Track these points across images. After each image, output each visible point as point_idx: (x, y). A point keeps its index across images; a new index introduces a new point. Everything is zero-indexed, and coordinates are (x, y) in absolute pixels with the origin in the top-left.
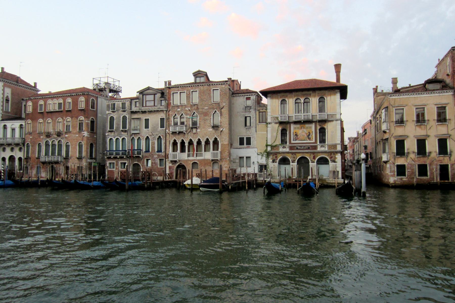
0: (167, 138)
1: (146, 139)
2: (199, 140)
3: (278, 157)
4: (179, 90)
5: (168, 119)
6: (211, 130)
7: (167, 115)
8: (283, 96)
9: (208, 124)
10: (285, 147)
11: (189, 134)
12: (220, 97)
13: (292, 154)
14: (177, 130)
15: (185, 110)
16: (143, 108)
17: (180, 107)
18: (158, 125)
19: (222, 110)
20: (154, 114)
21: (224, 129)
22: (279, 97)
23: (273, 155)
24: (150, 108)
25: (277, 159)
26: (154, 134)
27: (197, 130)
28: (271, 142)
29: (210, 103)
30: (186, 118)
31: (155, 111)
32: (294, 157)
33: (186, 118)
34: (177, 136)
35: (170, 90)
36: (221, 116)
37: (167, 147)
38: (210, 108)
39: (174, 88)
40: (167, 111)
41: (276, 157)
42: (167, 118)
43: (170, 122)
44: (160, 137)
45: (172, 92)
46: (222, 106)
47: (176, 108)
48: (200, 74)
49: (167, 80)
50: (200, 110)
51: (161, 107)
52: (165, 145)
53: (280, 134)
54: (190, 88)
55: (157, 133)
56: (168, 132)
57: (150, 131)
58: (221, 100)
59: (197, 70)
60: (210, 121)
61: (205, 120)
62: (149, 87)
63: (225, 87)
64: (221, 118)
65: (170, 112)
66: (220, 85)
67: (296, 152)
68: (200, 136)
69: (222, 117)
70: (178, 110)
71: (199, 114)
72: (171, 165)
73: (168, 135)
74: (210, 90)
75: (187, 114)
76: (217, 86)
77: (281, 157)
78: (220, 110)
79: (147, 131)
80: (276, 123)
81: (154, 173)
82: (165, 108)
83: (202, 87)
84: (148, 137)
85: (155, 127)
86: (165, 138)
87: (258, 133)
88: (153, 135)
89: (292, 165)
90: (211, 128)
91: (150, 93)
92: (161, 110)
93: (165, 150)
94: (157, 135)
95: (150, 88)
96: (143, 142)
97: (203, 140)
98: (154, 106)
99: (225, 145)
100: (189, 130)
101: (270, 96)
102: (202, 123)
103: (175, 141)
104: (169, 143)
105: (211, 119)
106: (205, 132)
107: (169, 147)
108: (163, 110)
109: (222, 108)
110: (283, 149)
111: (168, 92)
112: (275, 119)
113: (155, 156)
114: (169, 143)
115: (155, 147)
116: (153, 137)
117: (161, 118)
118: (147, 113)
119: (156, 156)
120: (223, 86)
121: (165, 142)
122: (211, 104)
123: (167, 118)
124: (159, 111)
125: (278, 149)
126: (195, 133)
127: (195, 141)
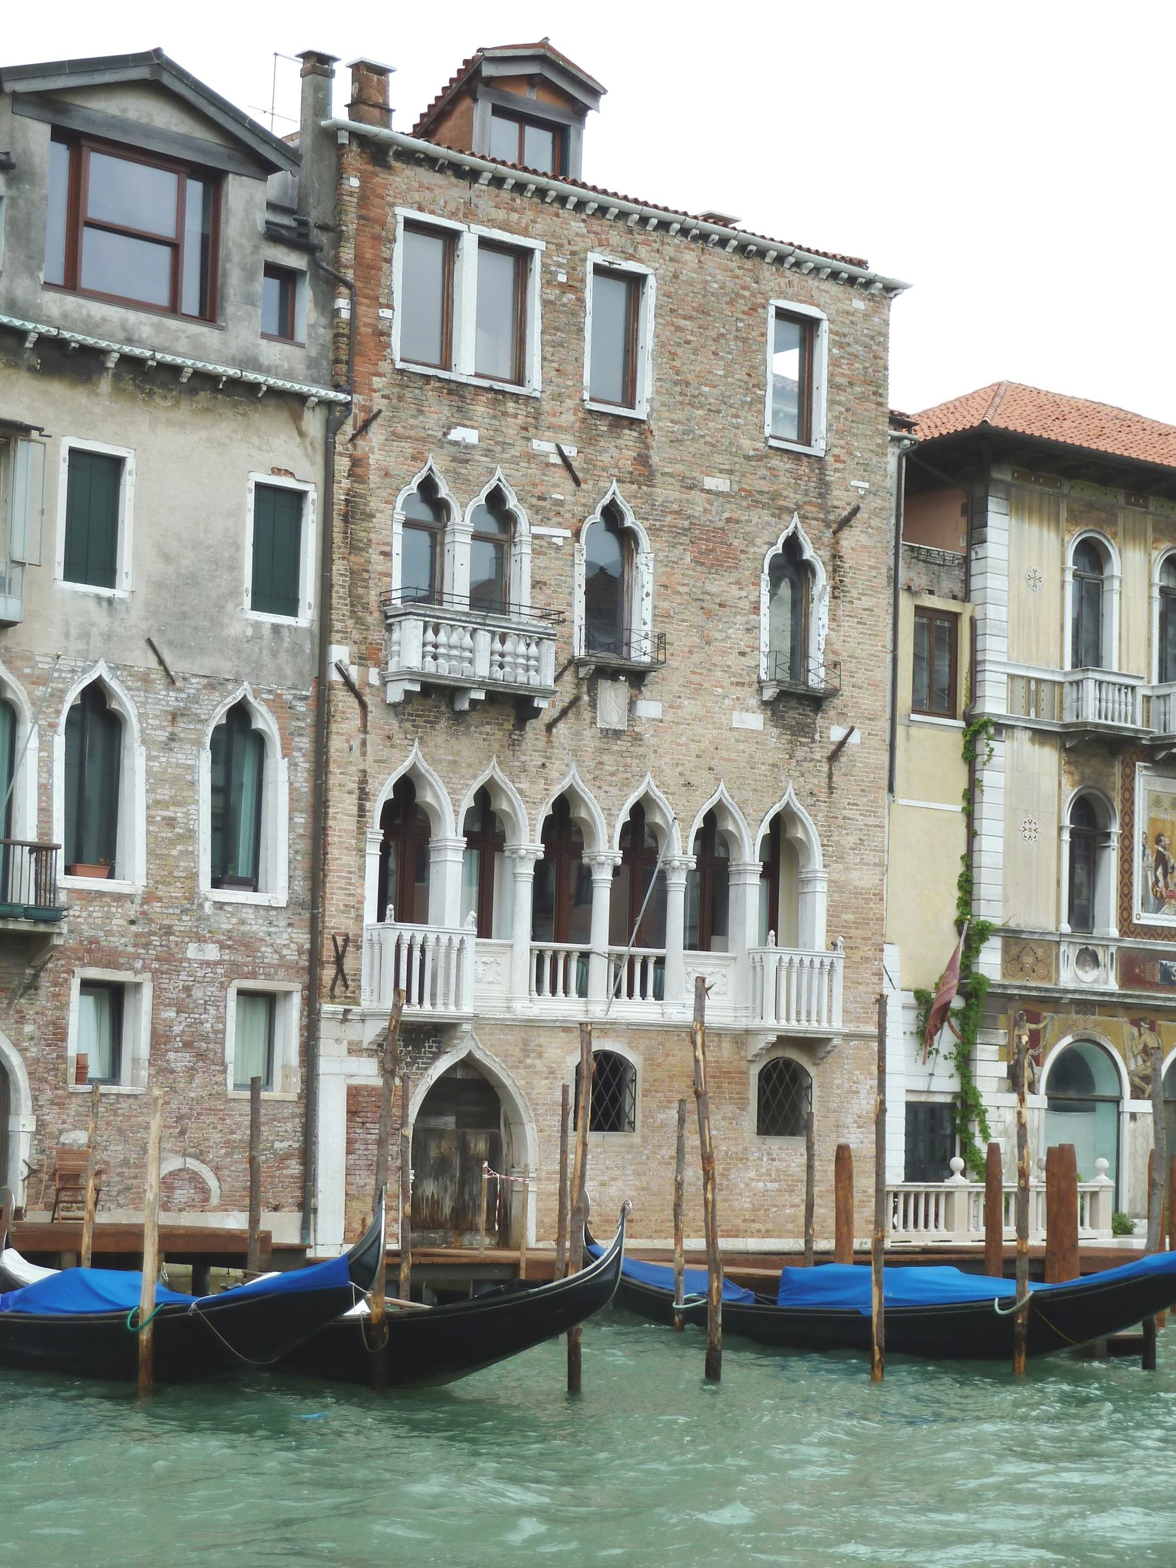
0: (336, 744)
1: (77, 722)
2: (638, 811)
3: (1048, 1037)
4: (469, 213)
5: (355, 511)
6: (755, 721)
7: (342, 464)
8: (1091, 506)
9: (733, 660)
10: (1096, 963)
11: (561, 728)
12: (832, 403)
13: (1136, 1023)
14: (482, 669)
15: (531, 457)
16: (56, 304)
17: (480, 409)
18: (234, 566)
19: (849, 540)
20: (184, 411)
21: (855, 738)
22: (1064, 514)
23: (1017, 1024)
24: (144, 325)
25: (1038, 1061)
26: (176, 666)
27: (632, 705)
28: (1005, 900)
29: (747, 445)
30: (542, 546)
31: (205, 381)
32: (1146, 1051)
33: (542, 546)
34: (440, 737)
35: (382, 178)
36: (837, 590)
37: (339, 857)
38: (753, 499)
39: (424, 175)
40: (334, 414)
41: (1035, 1038)
42: (339, 496)
43: (376, 558)
44: (240, 714)
45: (403, 212)
46: (841, 500)
47: (437, 411)
48: (531, 81)
49: (345, 54)
50: (665, 492)
51: (273, 352)
52: (300, 819)
53: (1066, 836)
54: (577, 226)
55: (225, 667)
56: (354, 672)
57: (136, 621)
58: (840, 434)
59: (524, 34)
60: (752, 629)
61: (709, 614)
62: (154, 59)
63: (866, 316)
64: (833, 619)
65: (376, 434)
66: (829, 286)
67: (1157, 1009)
68: (657, 772)
69: (843, 609)
70: (456, 434)
71: (653, 531)
72: (368, 1072)
73: (343, 701)
74: (754, 309)
75: (544, 510)
76: (812, 283)
77: (1067, 1040)
78: (829, 533)
79: (101, 618)
80: (1040, 736)
81: (173, 1163)
82: (315, 381)
83: (690, 257)
84: (96, 694)
85: (191, 580)
86: (305, 742)
87: (901, 801)
88: (171, 680)
89: (1133, 1116)
90: (753, 702)
91: (148, 131)
92: (270, 388)
93: (301, 886)
94: (214, 683)
95: (167, 80)
96: (45, 746)
97: (610, 816)
98: (174, 309)
99: (857, 893)
100: (567, 690)
101: (1008, 487)
102: (681, 638)
103: (406, 787)
104: (362, 811)
105: (756, 609)
106: (709, 734)
107: (361, 853)
108: (302, 398)
109: (845, 522)
110: (1080, 973)
111: (364, 198)
112: (1033, 700)
113: (192, 951)
114: (362, 811)
115: (190, 835)
116: (172, 700)
117: (259, 487)
118: (105, 385)
119: (212, 952)
120: (859, 304)
121: (304, 784)
122: (760, 458)
123: (339, 496)
124: (254, 387)
125: (1050, 965)
126: (618, 734)
127: (610, 816)
